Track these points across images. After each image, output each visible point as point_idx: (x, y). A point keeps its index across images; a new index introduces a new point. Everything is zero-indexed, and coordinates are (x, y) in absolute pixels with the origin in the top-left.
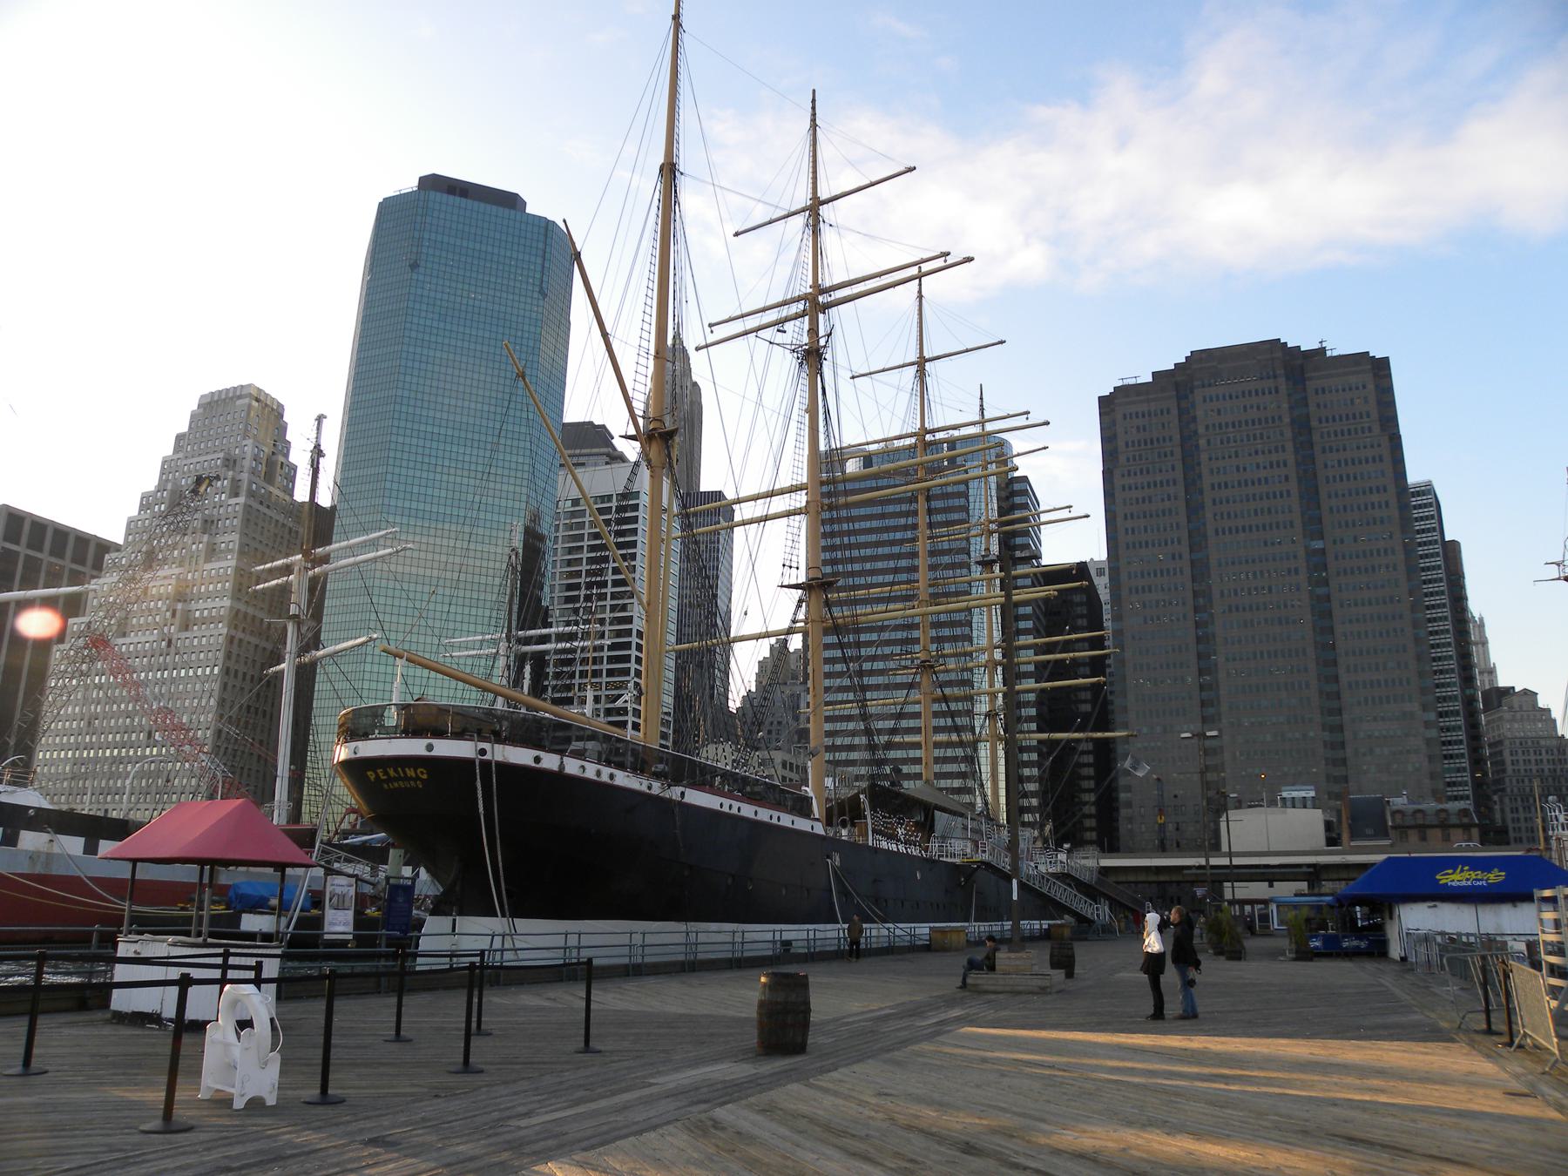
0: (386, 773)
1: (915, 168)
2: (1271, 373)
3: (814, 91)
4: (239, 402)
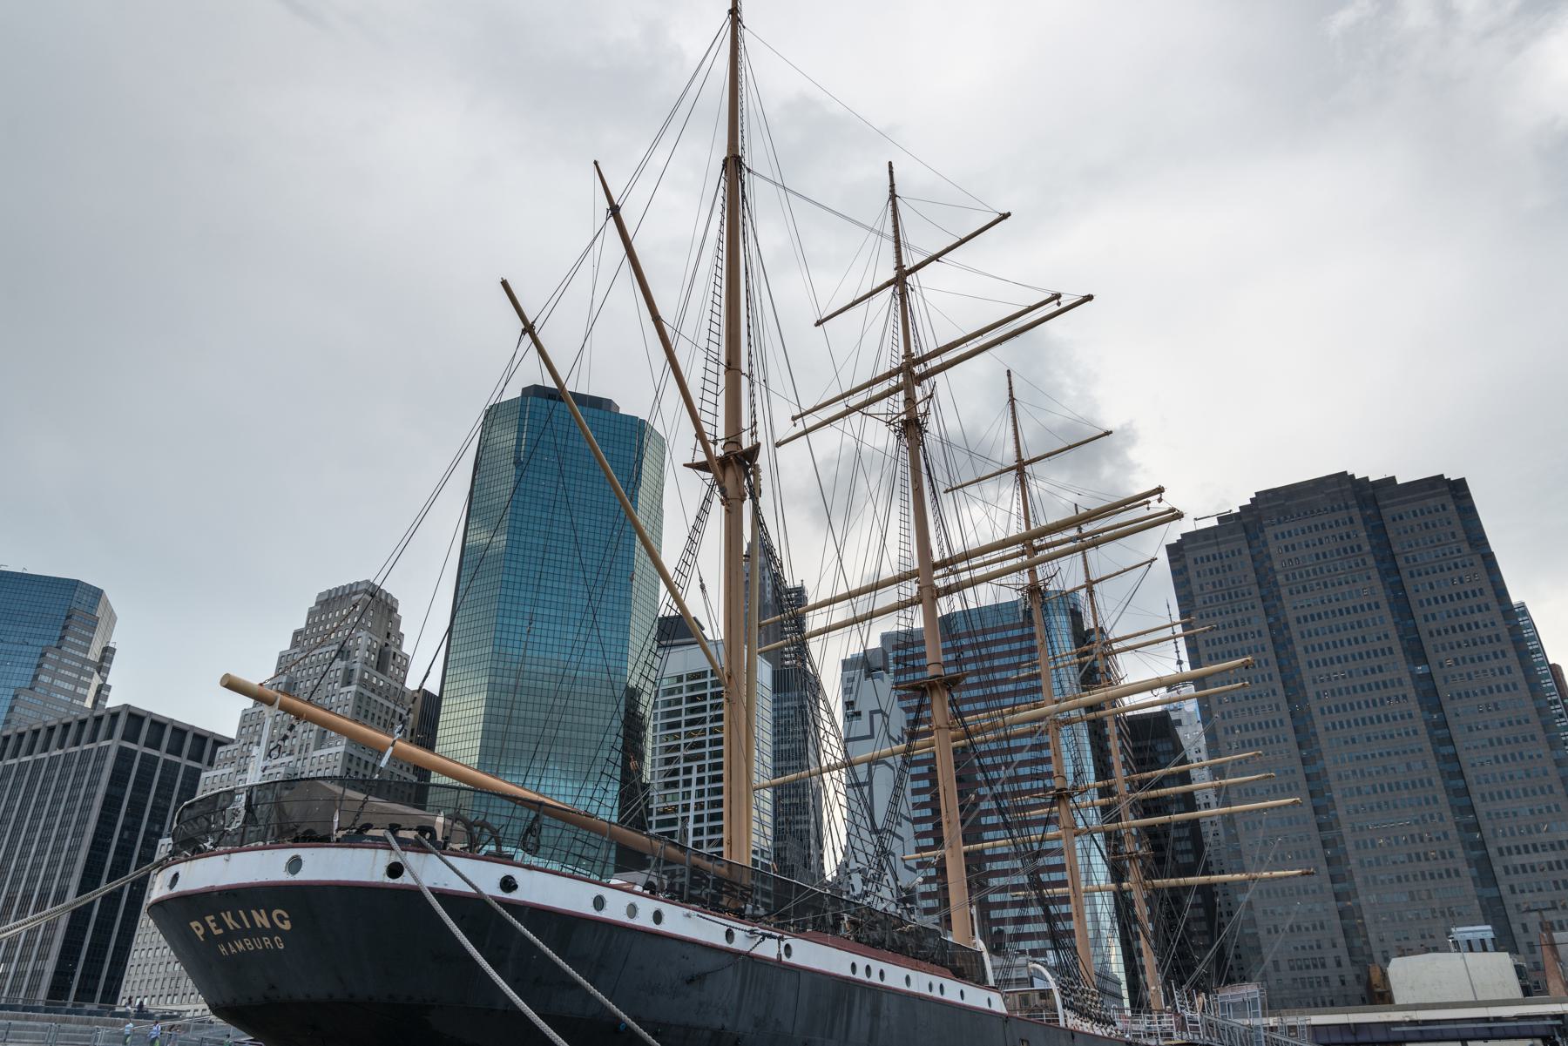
0: (221, 923)
1: (1009, 214)
2: (1343, 505)
3: (890, 163)
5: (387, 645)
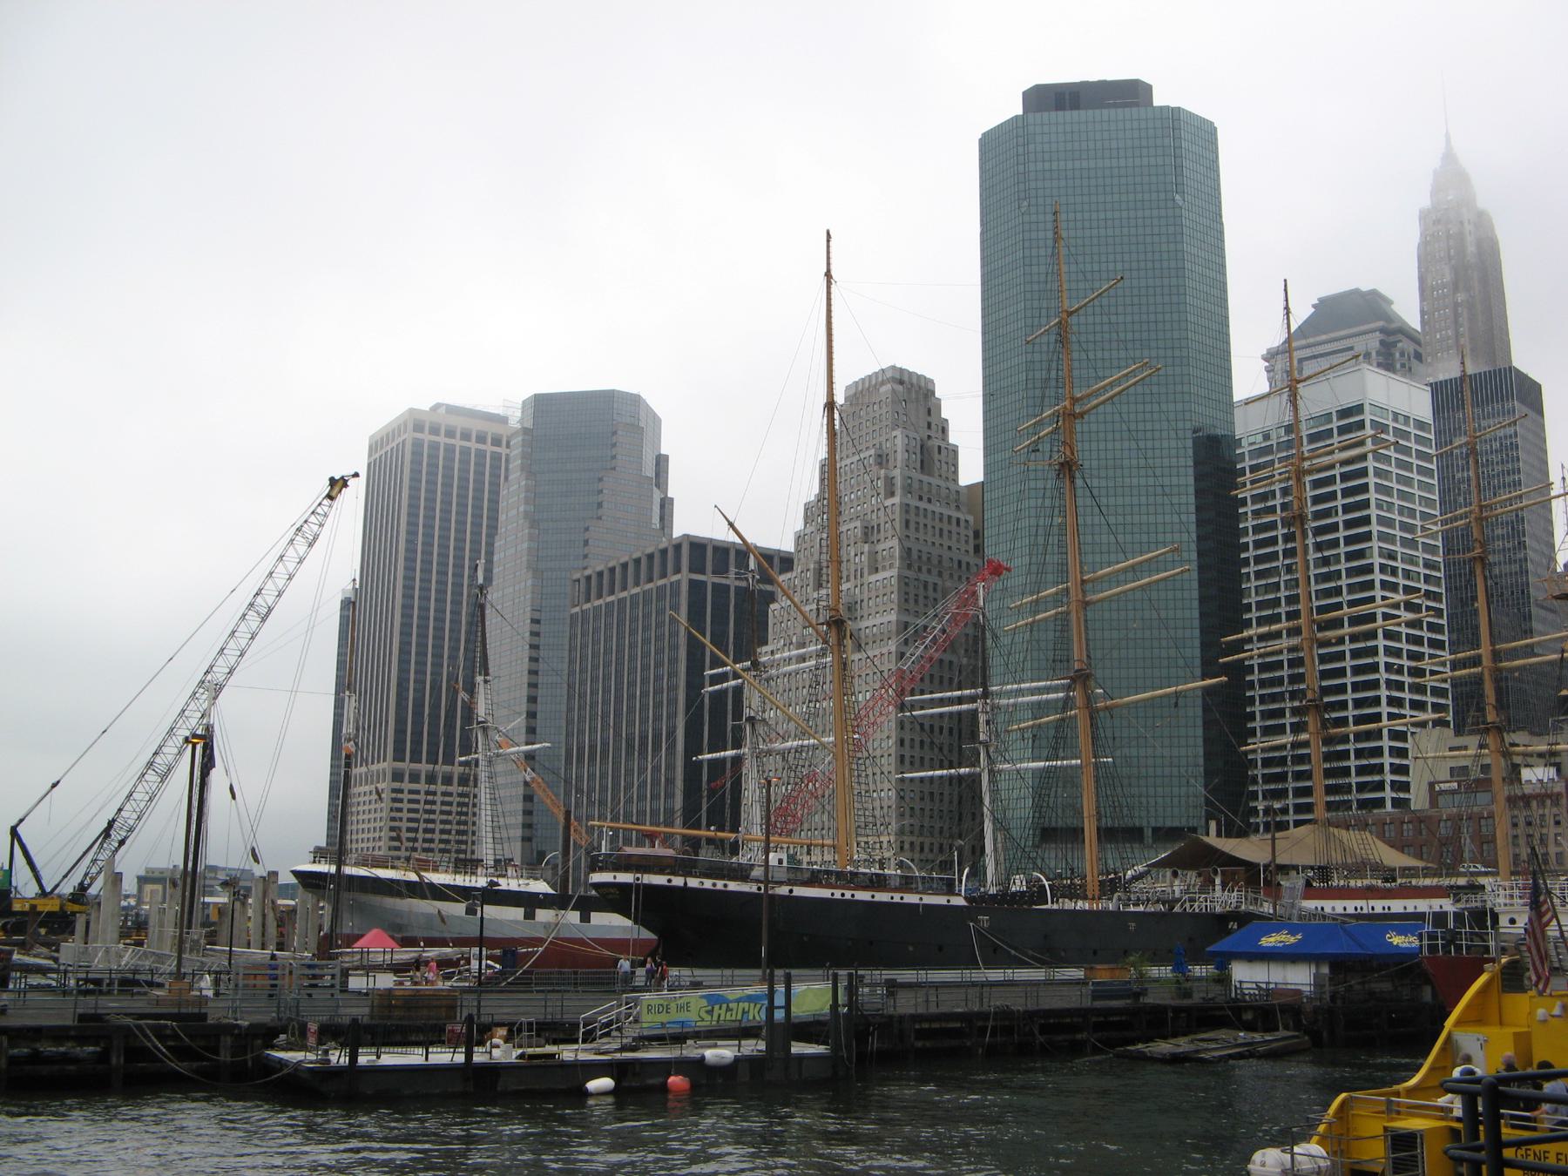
4: (883, 389)
5: (929, 437)
